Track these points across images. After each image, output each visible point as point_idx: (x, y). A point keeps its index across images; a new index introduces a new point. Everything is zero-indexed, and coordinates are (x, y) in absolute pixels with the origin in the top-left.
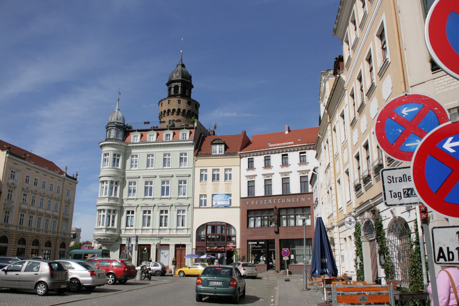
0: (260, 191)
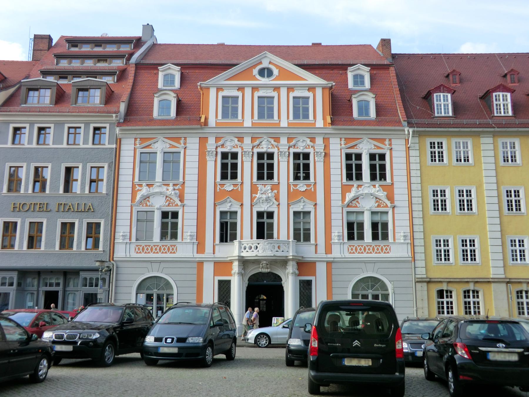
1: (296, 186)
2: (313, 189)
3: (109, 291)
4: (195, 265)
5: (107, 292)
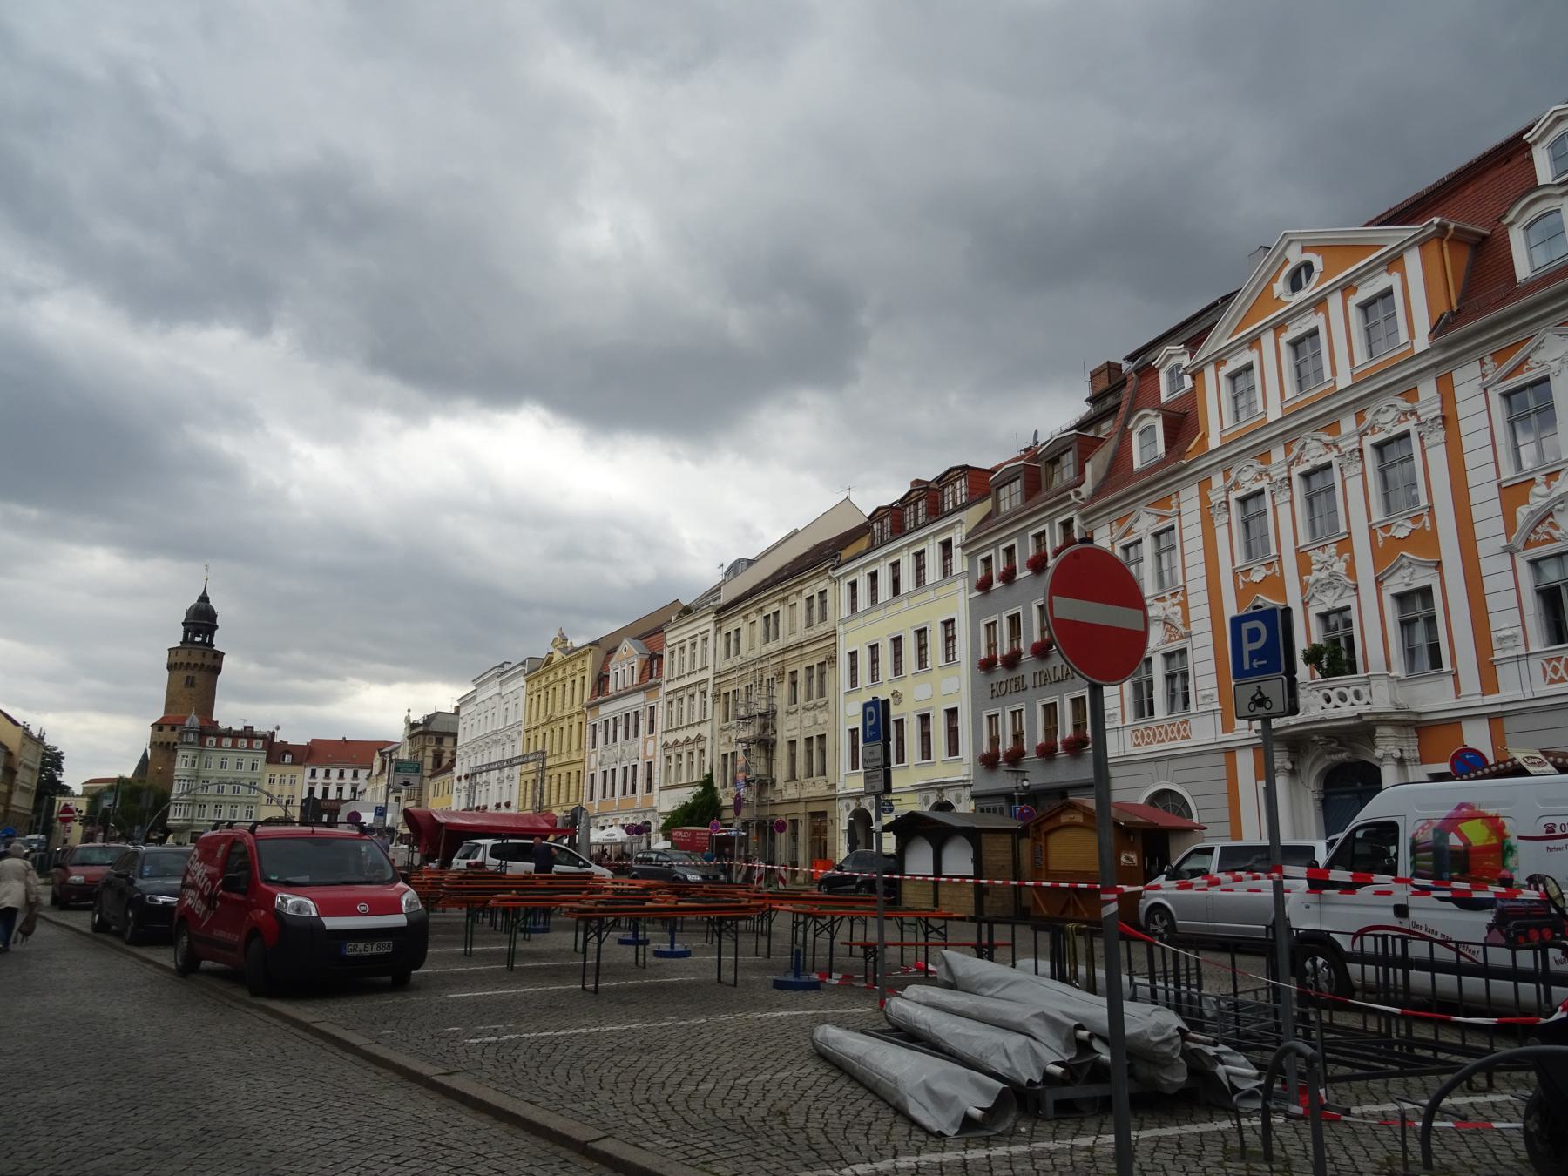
0: (318, 795)
1: (1386, 528)
2: (1428, 524)
4: (1221, 759)
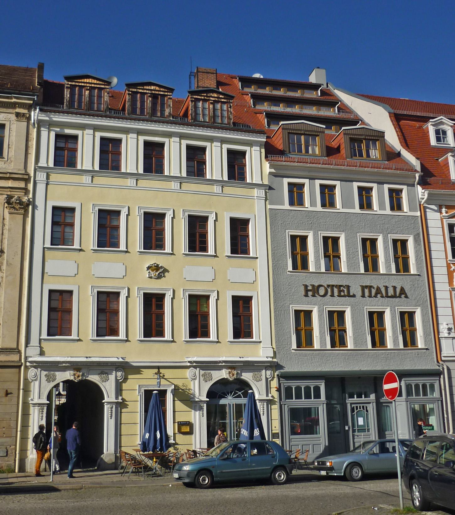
3: (442, 401)
5: (440, 402)
